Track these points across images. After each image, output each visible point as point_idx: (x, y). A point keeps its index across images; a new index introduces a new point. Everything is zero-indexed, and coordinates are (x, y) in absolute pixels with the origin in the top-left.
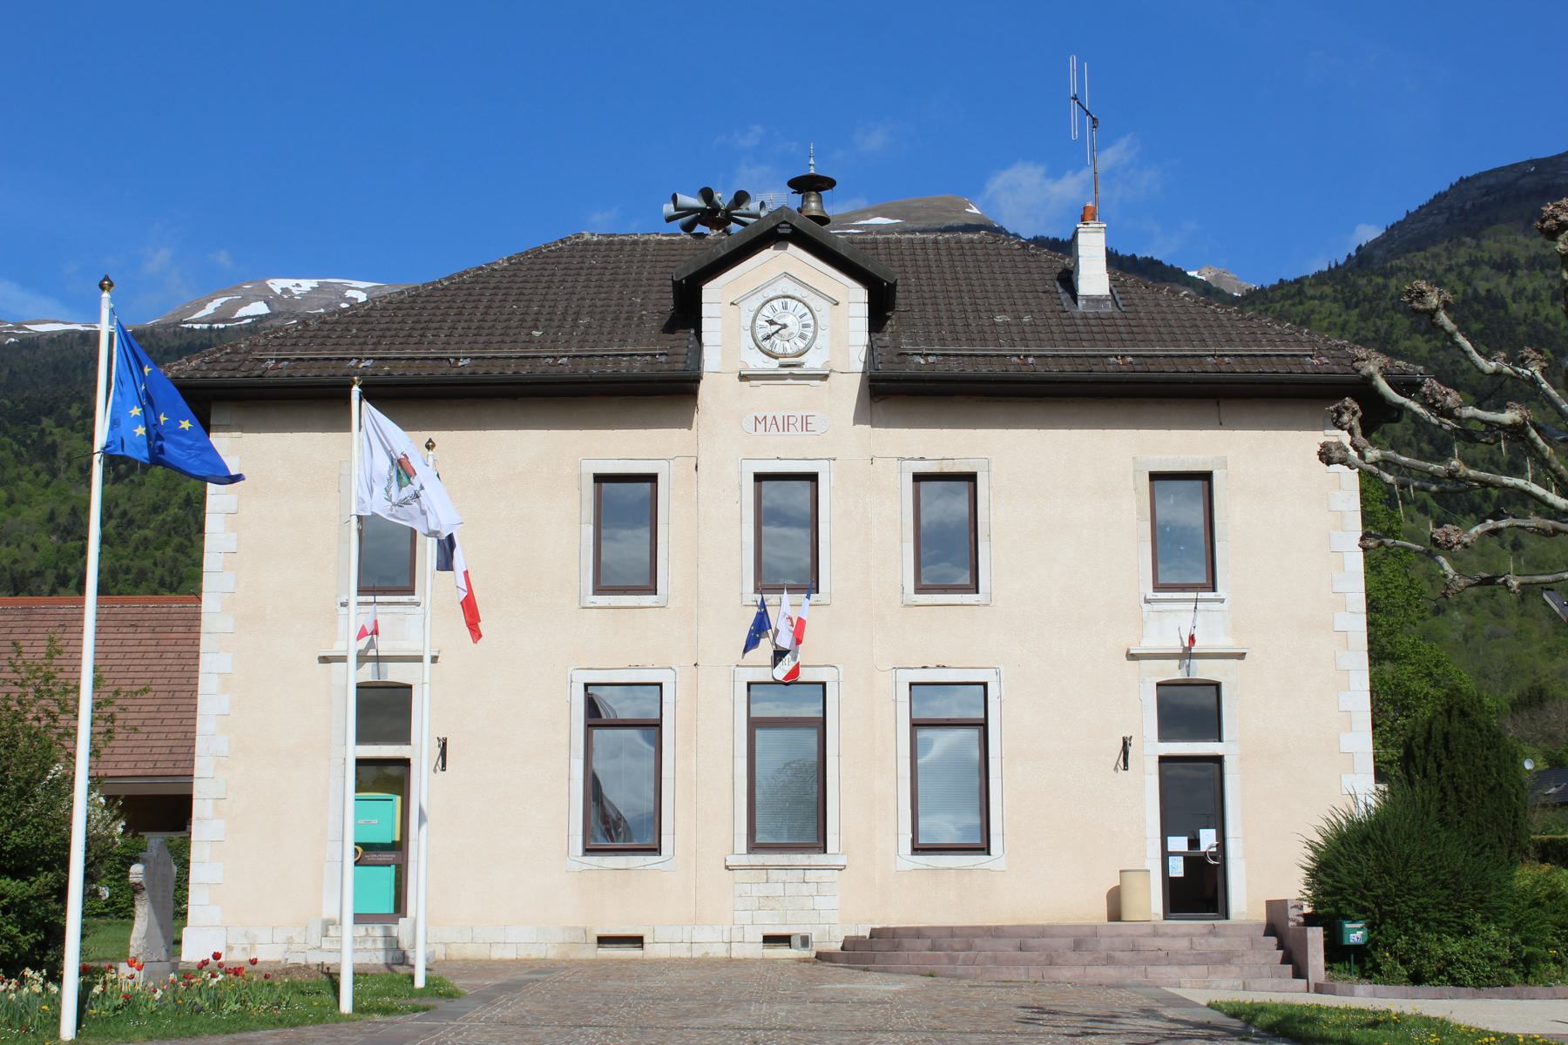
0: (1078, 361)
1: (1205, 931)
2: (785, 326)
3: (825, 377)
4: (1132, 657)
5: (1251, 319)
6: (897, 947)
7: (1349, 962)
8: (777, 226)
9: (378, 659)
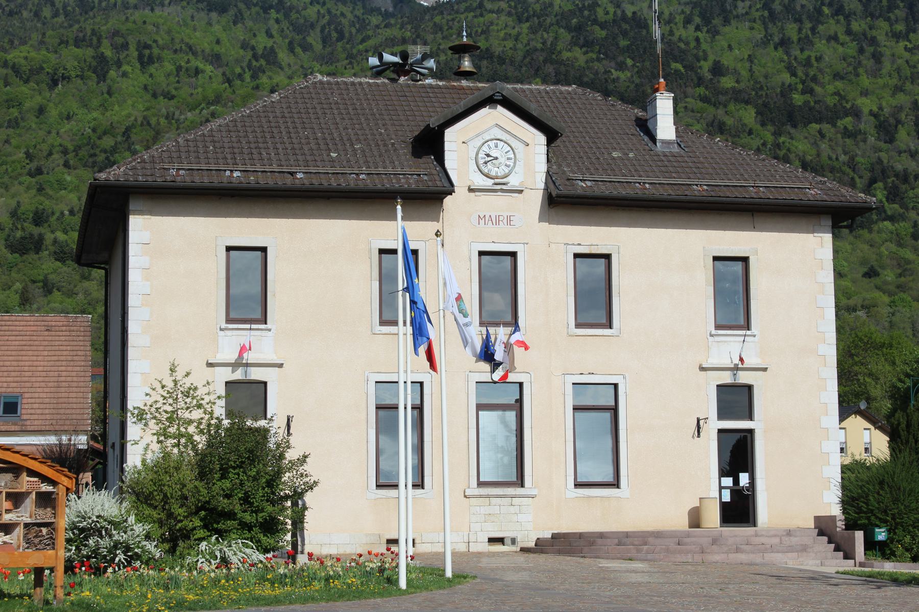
0: (675, 187)
1: (785, 533)
2: (496, 158)
3: (521, 192)
4: (702, 369)
5: (764, 160)
6: (592, 544)
7: (876, 550)
8: (494, 95)
9: (247, 365)
